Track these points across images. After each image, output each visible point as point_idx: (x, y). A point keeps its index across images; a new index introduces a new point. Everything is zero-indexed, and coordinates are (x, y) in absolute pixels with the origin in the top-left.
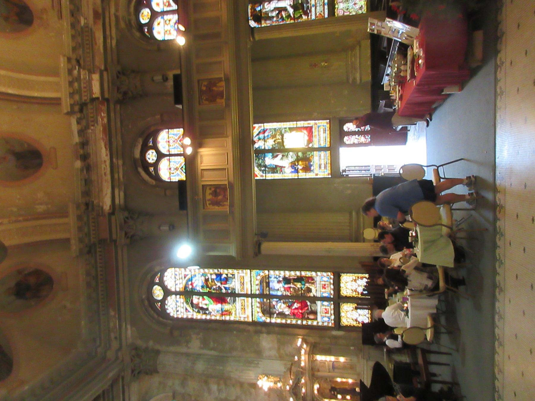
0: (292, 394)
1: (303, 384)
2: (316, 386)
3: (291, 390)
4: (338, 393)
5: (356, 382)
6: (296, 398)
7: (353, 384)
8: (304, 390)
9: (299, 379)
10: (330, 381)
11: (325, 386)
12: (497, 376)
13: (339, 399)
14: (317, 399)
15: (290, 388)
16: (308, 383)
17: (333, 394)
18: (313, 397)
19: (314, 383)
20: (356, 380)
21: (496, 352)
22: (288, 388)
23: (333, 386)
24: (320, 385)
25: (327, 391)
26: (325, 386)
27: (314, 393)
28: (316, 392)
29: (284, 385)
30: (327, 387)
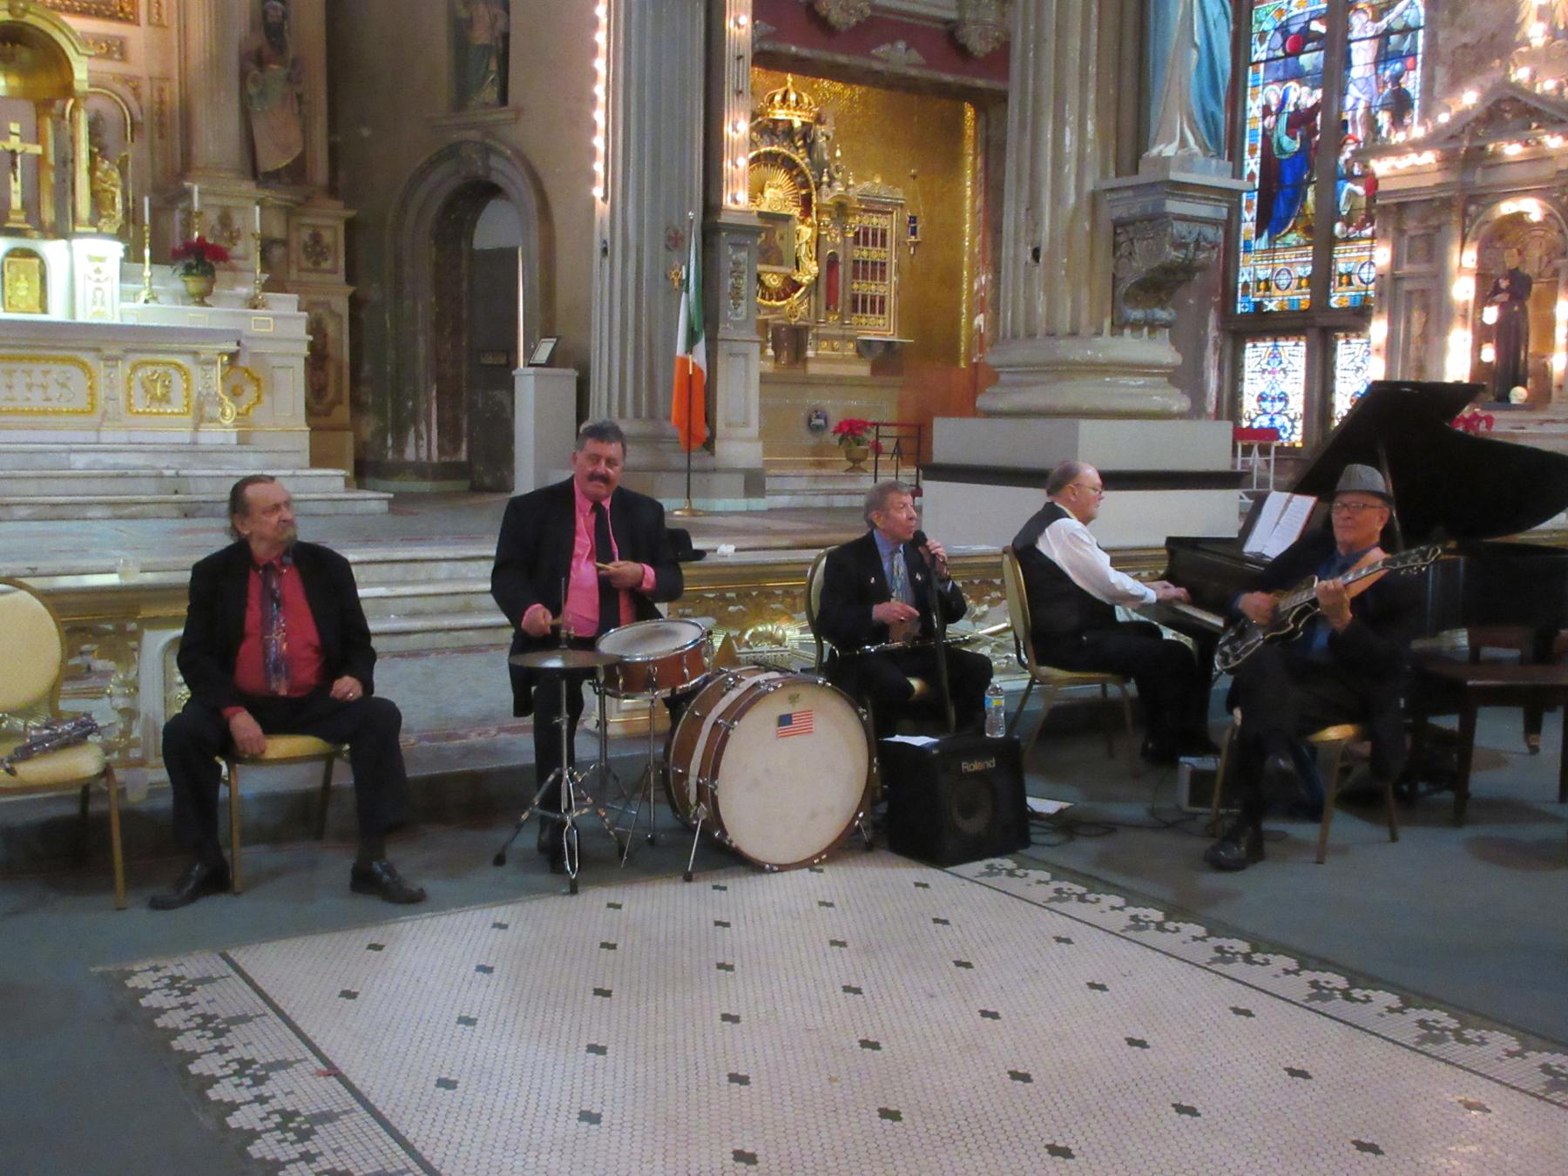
0: (1494, 98)
1: (1539, 143)
2: (1533, 208)
3: (1510, 93)
4: (1503, 306)
5: (1554, 390)
6: (1478, 120)
7: (1544, 373)
8: (1513, 150)
9: (1562, 122)
10: (1556, 273)
11: (1535, 253)
12: (1414, 1014)
13: (1482, 312)
14: (1478, 216)
15: (1516, 86)
16: (1546, 170)
17: (1497, 285)
18: (1484, 195)
19: (1545, 198)
20: (1560, 387)
21: (1526, 1047)
22: (1521, 74)
23: (1534, 286)
24: (1539, 223)
25: (1511, 260)
26: (1535, 253)
27: (1498, 202)
28: (1507, 208)
29: (1533, 57)
30: (1534, 260)
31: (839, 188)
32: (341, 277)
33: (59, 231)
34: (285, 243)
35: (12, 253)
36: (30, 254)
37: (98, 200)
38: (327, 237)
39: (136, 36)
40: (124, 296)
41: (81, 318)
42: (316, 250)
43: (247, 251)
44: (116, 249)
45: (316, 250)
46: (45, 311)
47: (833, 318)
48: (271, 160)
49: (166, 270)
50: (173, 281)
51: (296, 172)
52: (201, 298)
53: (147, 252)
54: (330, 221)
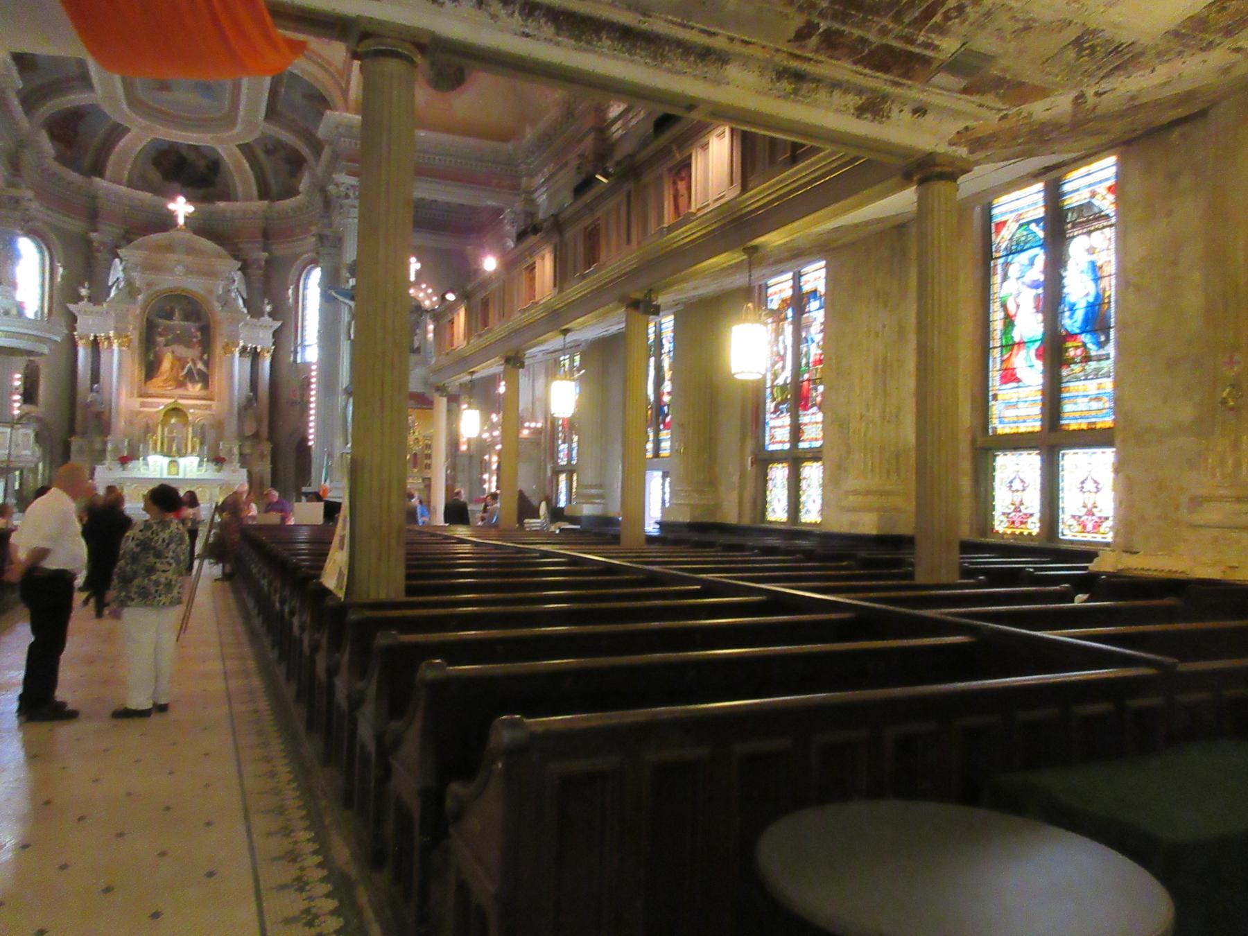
31: (416, 434)
32: (269, 462)
33: (184, 455)
34: (251, 454)
35: (171, 462)
36: (174, 461)
37: (193, 448)
38: (266, 453)
39: (214, 404)
40: (198, 470)
41: (187, 477)
42: (262, 456)
43: (236, 458)
44: (197, 459)
45: (262, 456)
46: (177, 474)
47: (416, 470)
48: (248, 433)
49: (210, 464)
50: (212, 466)
51: (256, 436)
52: (219, 471)
53: (205, 459)
54: (267, 447)
